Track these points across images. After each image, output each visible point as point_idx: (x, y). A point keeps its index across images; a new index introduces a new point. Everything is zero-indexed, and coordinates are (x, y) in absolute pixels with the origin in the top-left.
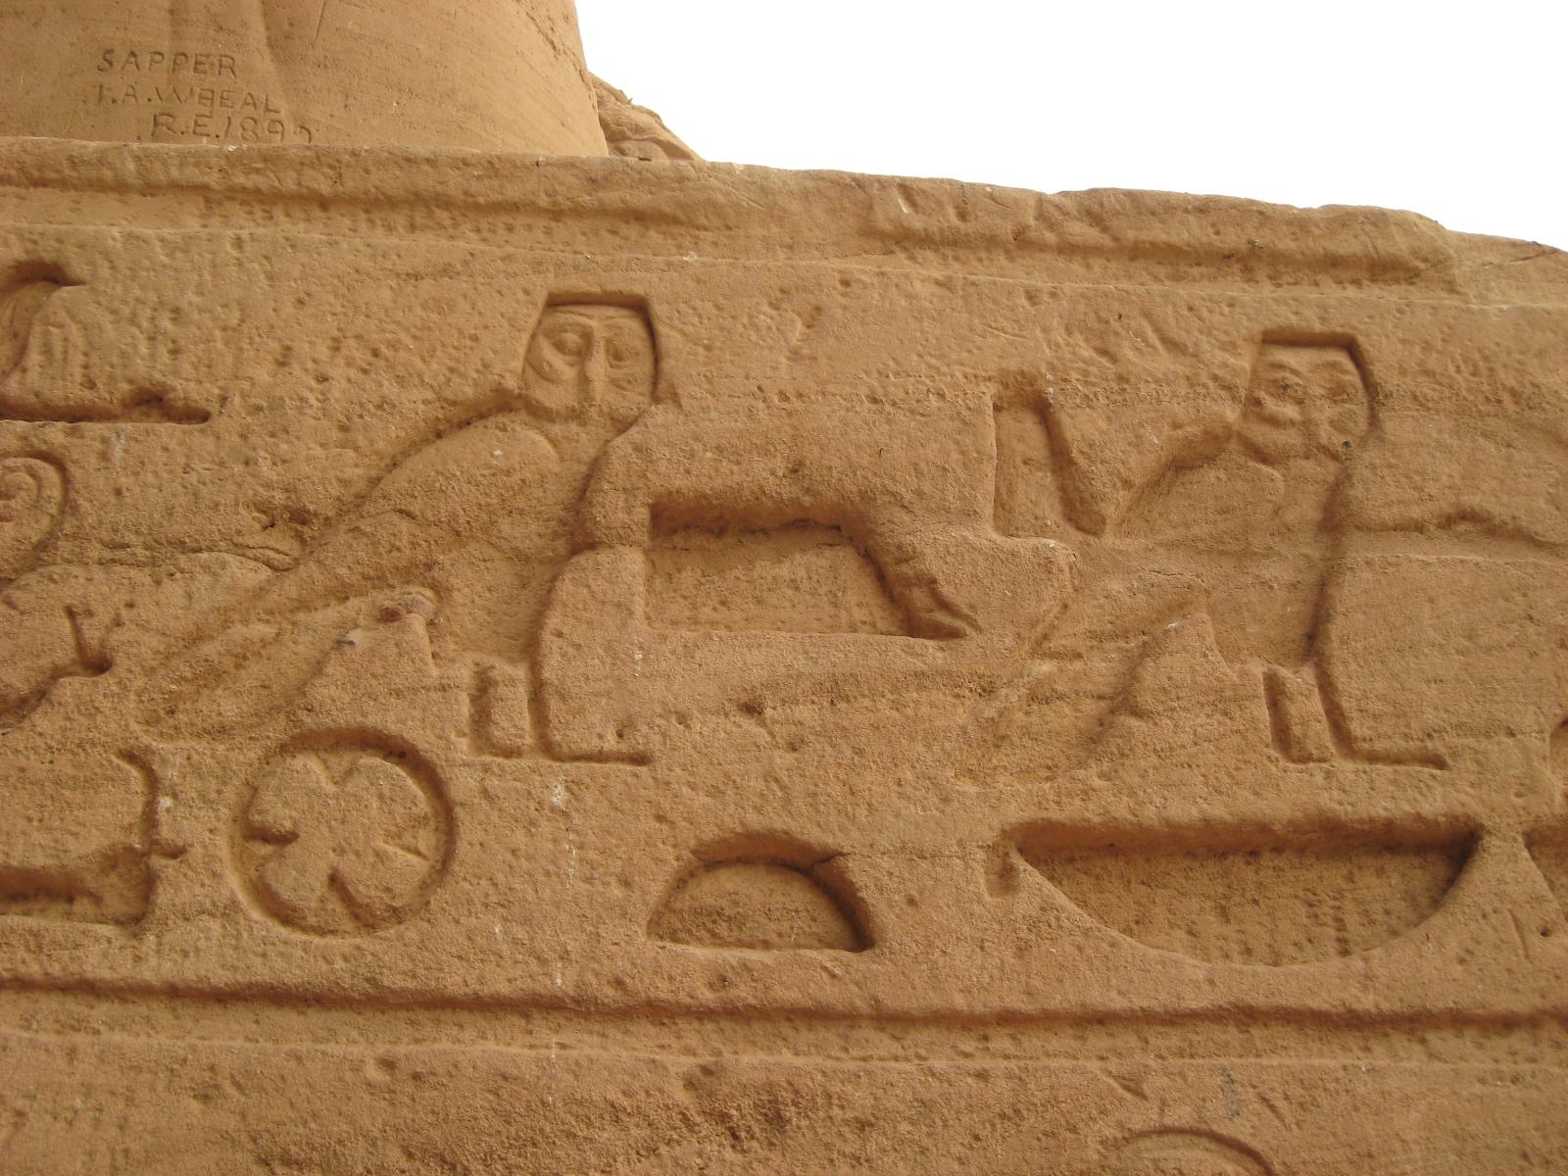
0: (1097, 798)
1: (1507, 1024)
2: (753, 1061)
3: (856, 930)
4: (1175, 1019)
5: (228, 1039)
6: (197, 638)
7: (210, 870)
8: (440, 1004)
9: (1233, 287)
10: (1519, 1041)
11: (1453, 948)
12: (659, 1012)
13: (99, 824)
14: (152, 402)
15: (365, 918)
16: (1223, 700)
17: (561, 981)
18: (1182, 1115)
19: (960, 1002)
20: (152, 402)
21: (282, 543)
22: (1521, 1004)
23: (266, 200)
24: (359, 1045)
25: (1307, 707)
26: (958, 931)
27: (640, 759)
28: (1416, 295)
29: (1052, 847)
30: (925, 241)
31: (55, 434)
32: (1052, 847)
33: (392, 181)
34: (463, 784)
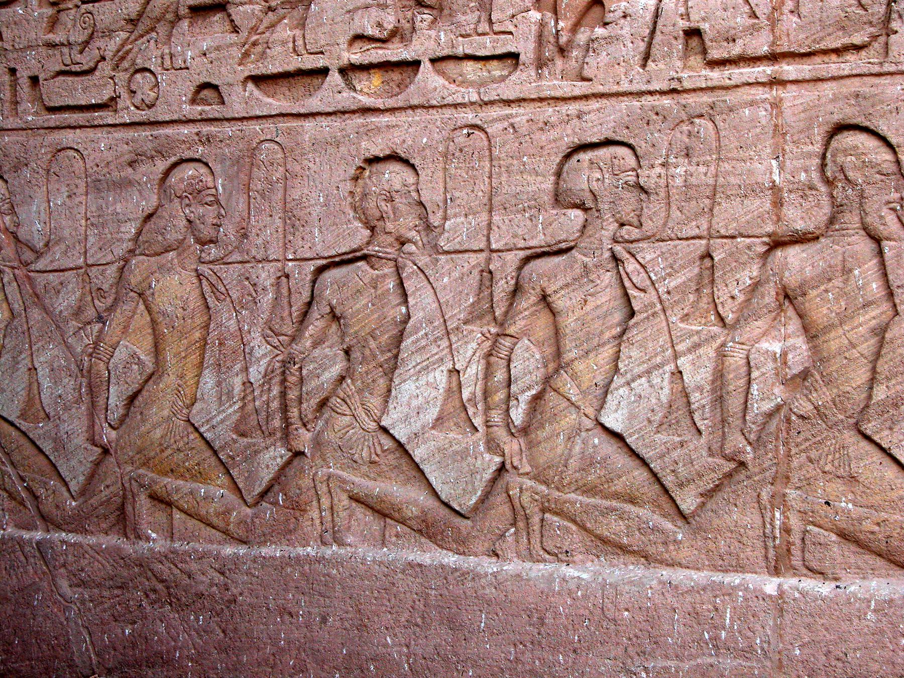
2: (206, 129)
5: (131, 133)
6: (118, 51)
7: (125, 101)
10: (333, 117)
11: (319, 98)
13: (107, 94)
17: (175, 117)
18: (269, 137)
19: (236, 115)
21: (130, 27)
22: (330, 110)
25: (300, 42)
26: (242, 99)
27: (187, 68)
29: (258, 80)
32: (258, 80)
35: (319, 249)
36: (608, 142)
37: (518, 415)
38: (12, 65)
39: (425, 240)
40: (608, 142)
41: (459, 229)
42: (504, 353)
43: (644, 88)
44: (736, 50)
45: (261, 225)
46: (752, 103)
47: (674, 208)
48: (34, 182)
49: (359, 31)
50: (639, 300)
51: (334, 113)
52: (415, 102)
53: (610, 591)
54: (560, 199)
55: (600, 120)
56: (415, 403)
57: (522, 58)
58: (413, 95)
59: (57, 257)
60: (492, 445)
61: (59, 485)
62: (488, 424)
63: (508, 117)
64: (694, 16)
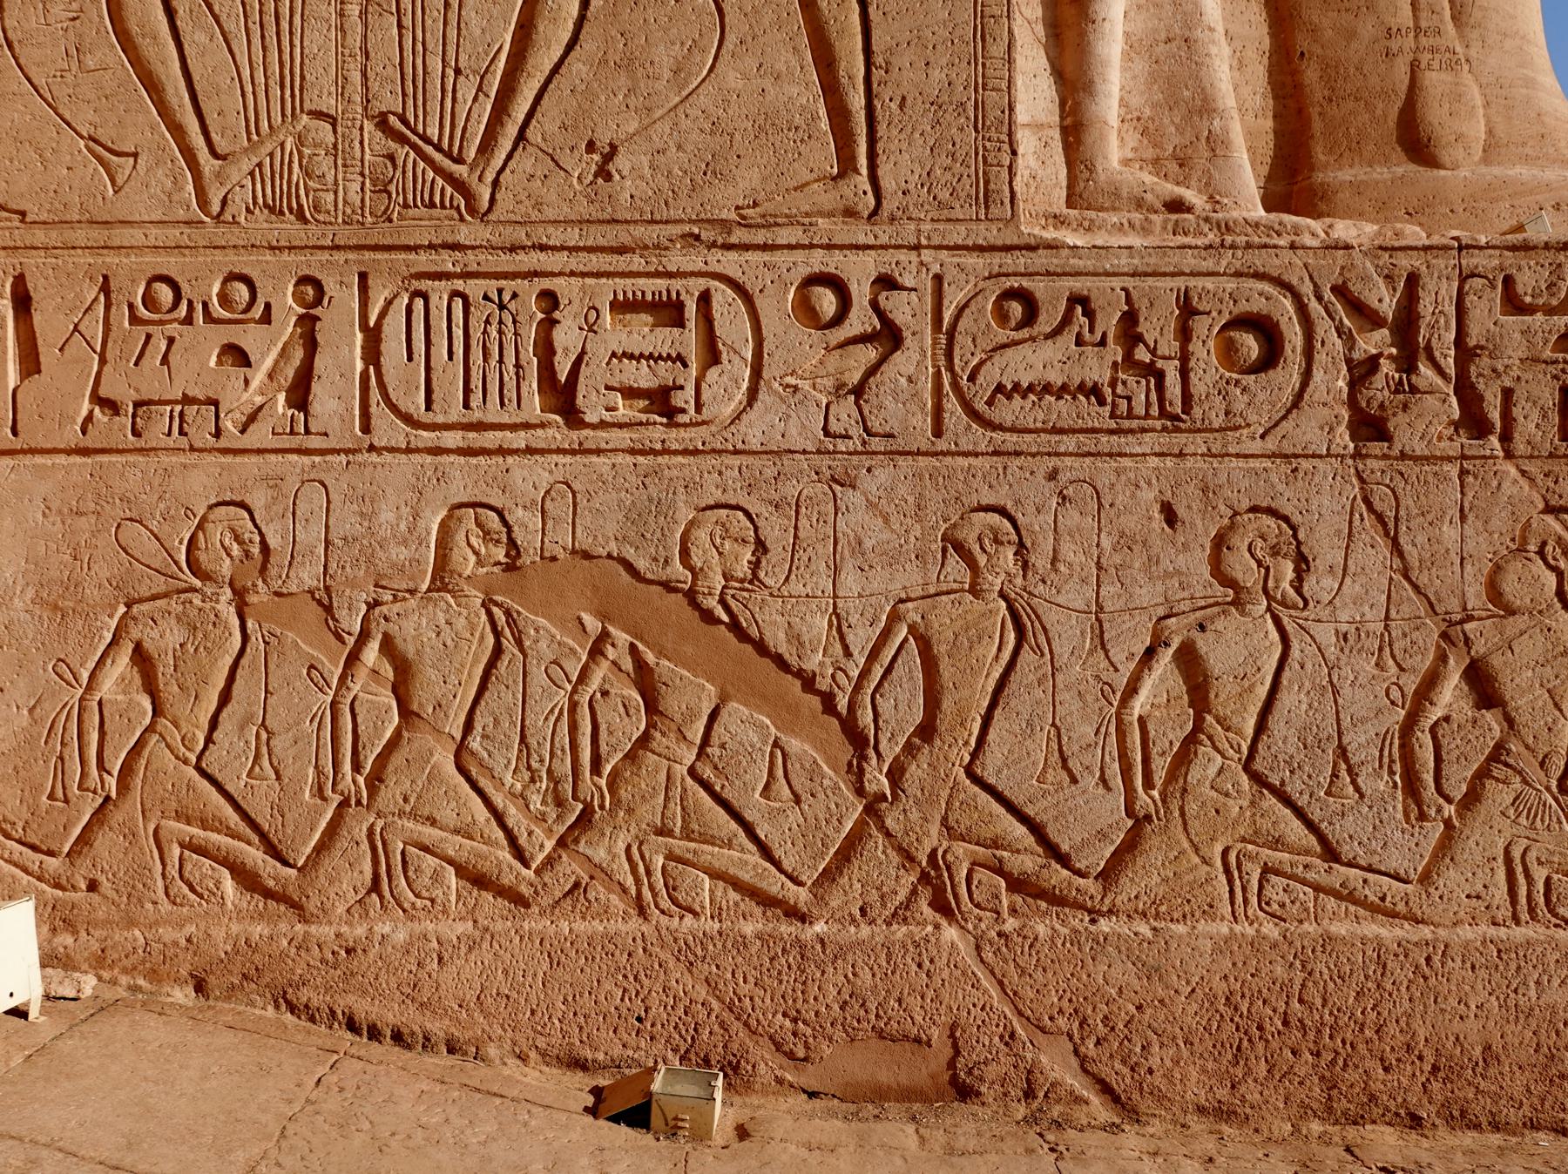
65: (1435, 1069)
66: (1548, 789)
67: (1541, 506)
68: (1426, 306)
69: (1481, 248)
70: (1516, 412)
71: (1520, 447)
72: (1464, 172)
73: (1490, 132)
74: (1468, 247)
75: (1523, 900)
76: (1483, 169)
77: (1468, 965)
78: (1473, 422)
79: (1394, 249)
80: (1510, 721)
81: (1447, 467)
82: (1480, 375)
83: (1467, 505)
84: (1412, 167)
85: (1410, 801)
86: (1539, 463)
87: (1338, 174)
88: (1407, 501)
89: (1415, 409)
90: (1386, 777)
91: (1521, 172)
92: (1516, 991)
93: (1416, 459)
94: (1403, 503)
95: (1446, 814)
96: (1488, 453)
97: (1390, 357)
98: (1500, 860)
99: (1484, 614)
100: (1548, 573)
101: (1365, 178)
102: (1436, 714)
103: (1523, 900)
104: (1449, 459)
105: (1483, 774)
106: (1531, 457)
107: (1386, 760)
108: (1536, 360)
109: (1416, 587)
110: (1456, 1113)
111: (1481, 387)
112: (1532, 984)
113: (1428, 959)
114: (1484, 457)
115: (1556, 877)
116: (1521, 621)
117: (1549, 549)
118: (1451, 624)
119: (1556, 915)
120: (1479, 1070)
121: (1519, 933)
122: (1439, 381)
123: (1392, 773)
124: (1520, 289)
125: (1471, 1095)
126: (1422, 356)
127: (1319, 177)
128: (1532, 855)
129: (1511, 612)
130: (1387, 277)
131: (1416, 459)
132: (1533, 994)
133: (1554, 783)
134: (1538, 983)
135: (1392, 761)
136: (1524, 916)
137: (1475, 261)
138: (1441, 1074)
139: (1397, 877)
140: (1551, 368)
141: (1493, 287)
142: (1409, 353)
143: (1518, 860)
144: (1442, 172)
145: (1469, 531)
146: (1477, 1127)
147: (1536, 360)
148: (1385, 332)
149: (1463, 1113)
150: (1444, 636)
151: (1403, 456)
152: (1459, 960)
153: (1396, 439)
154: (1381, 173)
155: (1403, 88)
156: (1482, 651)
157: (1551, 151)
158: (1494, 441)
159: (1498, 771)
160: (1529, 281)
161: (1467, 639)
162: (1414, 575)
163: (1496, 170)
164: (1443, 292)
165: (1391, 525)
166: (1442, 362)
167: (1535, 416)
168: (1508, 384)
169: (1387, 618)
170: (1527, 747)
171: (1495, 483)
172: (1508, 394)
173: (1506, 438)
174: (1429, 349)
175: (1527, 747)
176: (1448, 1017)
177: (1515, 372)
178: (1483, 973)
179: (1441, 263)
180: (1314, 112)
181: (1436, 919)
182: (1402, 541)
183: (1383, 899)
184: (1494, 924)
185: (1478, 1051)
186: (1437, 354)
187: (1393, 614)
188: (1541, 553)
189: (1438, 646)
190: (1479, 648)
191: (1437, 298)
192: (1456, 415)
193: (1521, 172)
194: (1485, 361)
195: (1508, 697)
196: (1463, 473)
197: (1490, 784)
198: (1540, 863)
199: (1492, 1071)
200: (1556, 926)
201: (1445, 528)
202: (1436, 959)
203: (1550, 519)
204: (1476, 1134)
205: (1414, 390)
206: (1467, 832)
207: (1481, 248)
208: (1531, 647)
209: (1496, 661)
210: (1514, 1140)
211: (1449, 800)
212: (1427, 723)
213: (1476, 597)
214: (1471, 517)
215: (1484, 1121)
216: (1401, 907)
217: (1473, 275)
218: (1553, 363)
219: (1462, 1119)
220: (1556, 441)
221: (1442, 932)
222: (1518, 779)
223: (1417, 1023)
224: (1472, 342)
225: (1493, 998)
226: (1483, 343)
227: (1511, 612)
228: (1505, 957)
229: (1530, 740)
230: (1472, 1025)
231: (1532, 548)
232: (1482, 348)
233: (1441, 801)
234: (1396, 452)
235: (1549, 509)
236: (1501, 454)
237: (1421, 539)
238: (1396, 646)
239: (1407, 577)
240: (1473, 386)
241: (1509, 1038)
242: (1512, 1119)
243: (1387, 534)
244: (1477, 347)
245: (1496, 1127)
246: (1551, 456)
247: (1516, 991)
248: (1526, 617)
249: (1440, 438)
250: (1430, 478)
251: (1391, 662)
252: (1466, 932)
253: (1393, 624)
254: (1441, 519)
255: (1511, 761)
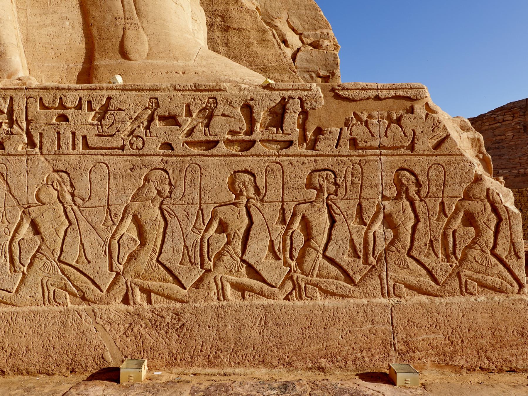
0: (190, 139)
1: (219, 156)
3: (173, 149)
4: (194, 155)
5: (130, 158)
8: (144, 155)
9: (207, 93)
12: (159, 155)
14: (120, 110)
15: (139, 150)
16: (201, 131)
20: (120, 110)
23: (127, 90)
24: (139, 158)
28: (223, 93)
30: (180, 90)
31: (113, 112)
33: (136, 87)
34: (145, 139)
35: (216, 199)
36: (325, 170)
37: (296, 254)
38: (74, 130)
39: (258, 198)
40: (325, 170)
41: (274, 193)
42: (290, 234)
43: (337, 154)
44: (368, 145)
45: (190, 192)
46: (373, 160)
47: (348, 190)
48: (83, 174)
49: (232, 129)
50: (337, 218)
51: (221, 156)
52: (254, 153)
53: (336, 309)
54: (310, 185)
55: (322, 163)
56: (257, 251)
57: (294, 142)
58: (253, 151)
59: (95, 201)
60: (286, 263)
61: (95, 288)
62: (284, 257)
63: (289, 160)
64: (353, 134)
65: (11, 354)
66: (54, 261)
67: (52, 170)
68: (16, 107)
69: (32, 89)
70: (43, 140)
71: (45, 151)
72: (138, 62)
73: (150, 49)
74: (28, 89)
75: (46, 297)
76: (146, 61)
77: (24, 320)
78: (31, 144)
79: (5, 89)
80: (43, 239)
81: (22, 158)
82: (32, 129)
83: (28, 170)
84: (123, 60)
85: (12, 266)
86: (51, 156)
87: (100, 62)
88: (10, 169)
89: (12, 140)
90: (3, 258)
91: (158, 62)
92: (38, 328)
93: (13, 155)
94: (8, 169)
95: (22, 270)
96: (34, 153)
97: (6, 123)
98: (40, 284)
99: (34, 205)
100: (54, 191)
101: (108, 63)
102: (19, 238)
103: (46, 297)
104: (23, 155)
105: (34, 256)
106: (48, 154)
107: (4, 253)
108: (49, 124)
109: (13, 196)
110: (16, 369)
111: (32, 133)
112: (43, 325)
113: (11, 318)
114: (33, 155)
115: (57, 289)
116: (46, 207)
117: (55, 184)
118: (25, 208)
119: (56, 302)
120: (24, 354)
121: (45, 308)
122: (20, 131)
123: (5, 257)
124: (44, 102)
125: (21, 363)
126: (15, 123)
127: (96, 63)
128: (49, 282)
129: (43, 204)
130: (3, 98)
131: (13, 155)
132: (43, 328)
133: (56, 259)
134: (45, 325)
135: (5, 253)
136: (47, 302)
137: (30, 93)
138: (12, 356)
139: (7, 291)
140: (53, 126)
141: (36, 101)
142: (12, 122)
143: (45, 284)
144: (131, 62)
145: (29, 178)
146: (22, 374)
147: (49, 124)
148: (6, 115)
149: (18, 369)
150: (23, 212)
151: (9, 155)
152: (21, 318)
153: (6, 149)
154: (113, 62)
155: (121, 35)
156: (34, 217)
157: (171, 55)
158: (37, 150)
159: (39, 255)
160: (47, 99)
161: (29, 213)
162: (13, 192)
163: (150, 61)
164: (21, 103)
165: (5, 176)
166: (20, 124)
167: (50, 142)
168: (41, 131)
169: (5, 206)
170: (48, 247)
171: (37, 163)
172: (41, 134)
173: (41, 148)
174: (16, 120)
175: (48, 247)
176: (15, 337)
177: (43, 128)
178: (28, 322)
179: (20, 94)
180: (96, 42)
181: (19, 304)
182: (8, 181)
183: (3, 298)
184: (38, 305)
185: (25, 348)
186: (19, 122)
187: (6, 205)
188: (52, 185)
189: (21, 215)
190: (33, 216)
191: (19, 105)
192: (26, 141)
193: (158, 62)
194: (33, 124)
195: (42, 232)
196: (28, 159)
197: (36, 259)
198: (52, 285)
199: (28, 355)
200: (56, 305)
201: (22, 177)
202: (14, 318)
203: (56, 174)
204: (20, 376)
205: (12, 133)
206: (29, 275)
207: (32, 89)
208: (49, 215)
209: (38, 220)
210: (32, 377)
211: (24, 266)
212: (17, 241)
213: (33, 199)
214: (30, 174)
215: (24, 371)
216: (8, 301)
217: (30, 97)
218: (55, 125)
219: (18, 371)
220: (56, 149)
221: (18, 309)
222: (45, 258)
223: (6, 340)
224: (29, 118)
225: (31, 331)
226: (33, 118)
227: (43, 204)
228: (35, 316)
229: (49, 245)
230: (23, 340)
231: (50, 183)
232: (33, 120)
233: (21, 265)
234: (6, 153)
235: (54, 171)
236: (39, 154)
237: (15, 181)
238: (7, 215)
239: (11, 193)
240: (30, 132)
241: (34, 344)
242: (33, 371)
243: (4, 179)
244: (31, 120)
245: (28, 373)
246: (54, 154)
247: (38, 328)
248: (48, 205)
249: (23, 148)
250: (17, 162)
251: (6, 221)
252: (24, 309)
253: (6, 208)
254: (20, 174)
255: (43, 252)
